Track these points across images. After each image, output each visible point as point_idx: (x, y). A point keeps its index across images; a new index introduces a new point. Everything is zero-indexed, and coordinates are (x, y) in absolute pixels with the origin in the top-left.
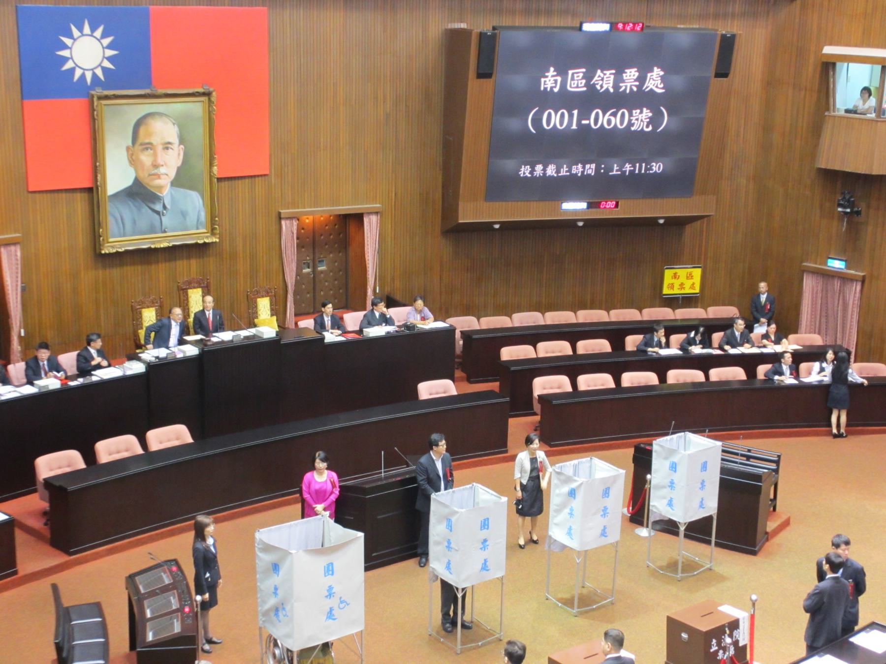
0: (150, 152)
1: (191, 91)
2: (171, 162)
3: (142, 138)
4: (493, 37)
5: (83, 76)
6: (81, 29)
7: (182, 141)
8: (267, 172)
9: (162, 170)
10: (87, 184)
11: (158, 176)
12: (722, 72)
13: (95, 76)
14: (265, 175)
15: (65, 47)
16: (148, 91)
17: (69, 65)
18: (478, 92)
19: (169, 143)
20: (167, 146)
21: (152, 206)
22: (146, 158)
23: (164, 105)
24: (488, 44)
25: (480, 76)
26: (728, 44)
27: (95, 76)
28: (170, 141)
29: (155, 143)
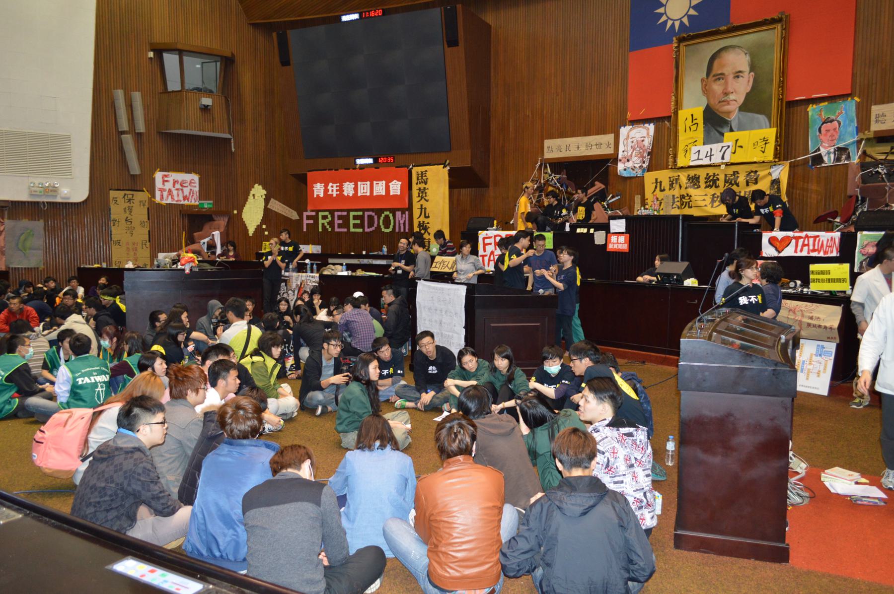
0: (722, 81)
2: (740, 89)
3: (716, 70)
7: (752, 68)
8: (849, 92)
9: (732, 97)
11: (728, 104)
13: (682, 23)
19: (740, 72)
20: (738, 75)
21: (720, 130)
22: (717, 88)
23: (738, 38)
27: (682, 23)
28: (741, 69)
29: (727, 74)
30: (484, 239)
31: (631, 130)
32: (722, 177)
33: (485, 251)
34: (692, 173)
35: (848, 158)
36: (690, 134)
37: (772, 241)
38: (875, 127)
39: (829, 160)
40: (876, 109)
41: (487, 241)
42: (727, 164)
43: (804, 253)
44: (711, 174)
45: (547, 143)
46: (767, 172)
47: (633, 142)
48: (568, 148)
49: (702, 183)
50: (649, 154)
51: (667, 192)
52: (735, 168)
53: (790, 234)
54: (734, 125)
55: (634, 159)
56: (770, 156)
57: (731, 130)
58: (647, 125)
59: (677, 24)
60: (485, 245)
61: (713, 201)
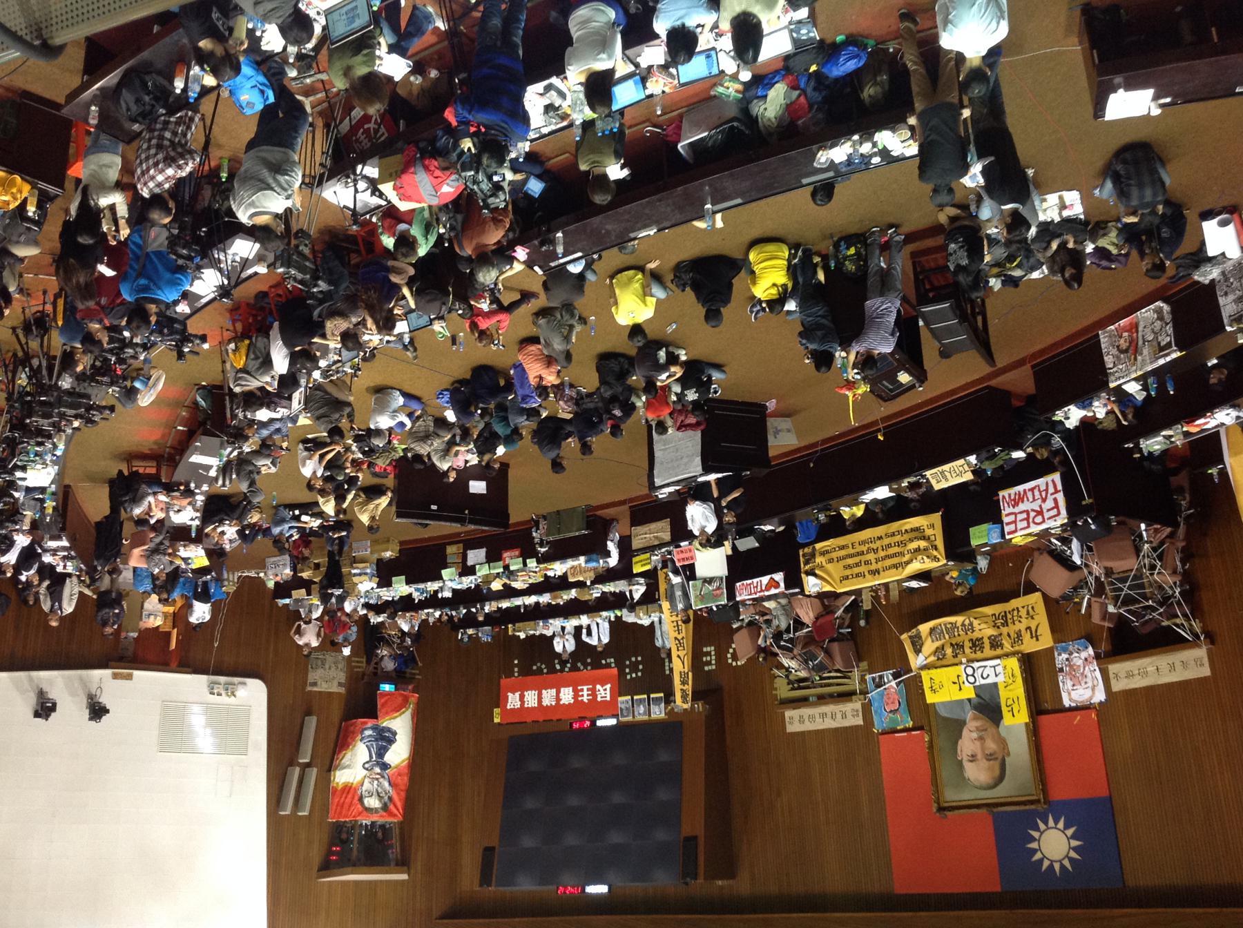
1: (956, 812)
2: (968, 743)
3: (996, 765)
4: (684, 877)
5: (1056, 822)
6: (1062, 867)
7: (960, 764)
9: (975, 735)
10: (1044, 720)
11: (978, 729)
12: (489, 850)
13: (1046, 823)
14: (882, 734)
15: (1075, 849)
16: (995, 810)
17: (1070, 832)
18: (694, 822)
20: (973, 758)
22: (991, 746)
24: (689, 872)
25: (695, 838)
26: (485, 879)
27: (1046, 823)
30: (1059, 514)
31: (1091, 698)
32: (967, 651)
33: (1055, 500)
34: (999, 652)
35: (874, 679)
36: (1011, 695)
37: (777, 585)
38: (856, 705)
39: (888, 675)
40: (859, 721)
41: (1054, 512)
42: (961, 663)
43: (755, 580)
44: (979, 653)
45: (1206, 671)
46: (929, 660)
47: (1083, 683)
48: (1172, 667)
49: (986, 641)
50: (1061, 670)
51: (1022, 627)
52: (956, 661)
53: (767, 593)
54: (968, 707)
55: (1080, 662)
56: (925, 675)
57: (969, 700)
58: (1073, 705)
59: (1051, 823)
60: (1057, 506)
61: (971, 624)
